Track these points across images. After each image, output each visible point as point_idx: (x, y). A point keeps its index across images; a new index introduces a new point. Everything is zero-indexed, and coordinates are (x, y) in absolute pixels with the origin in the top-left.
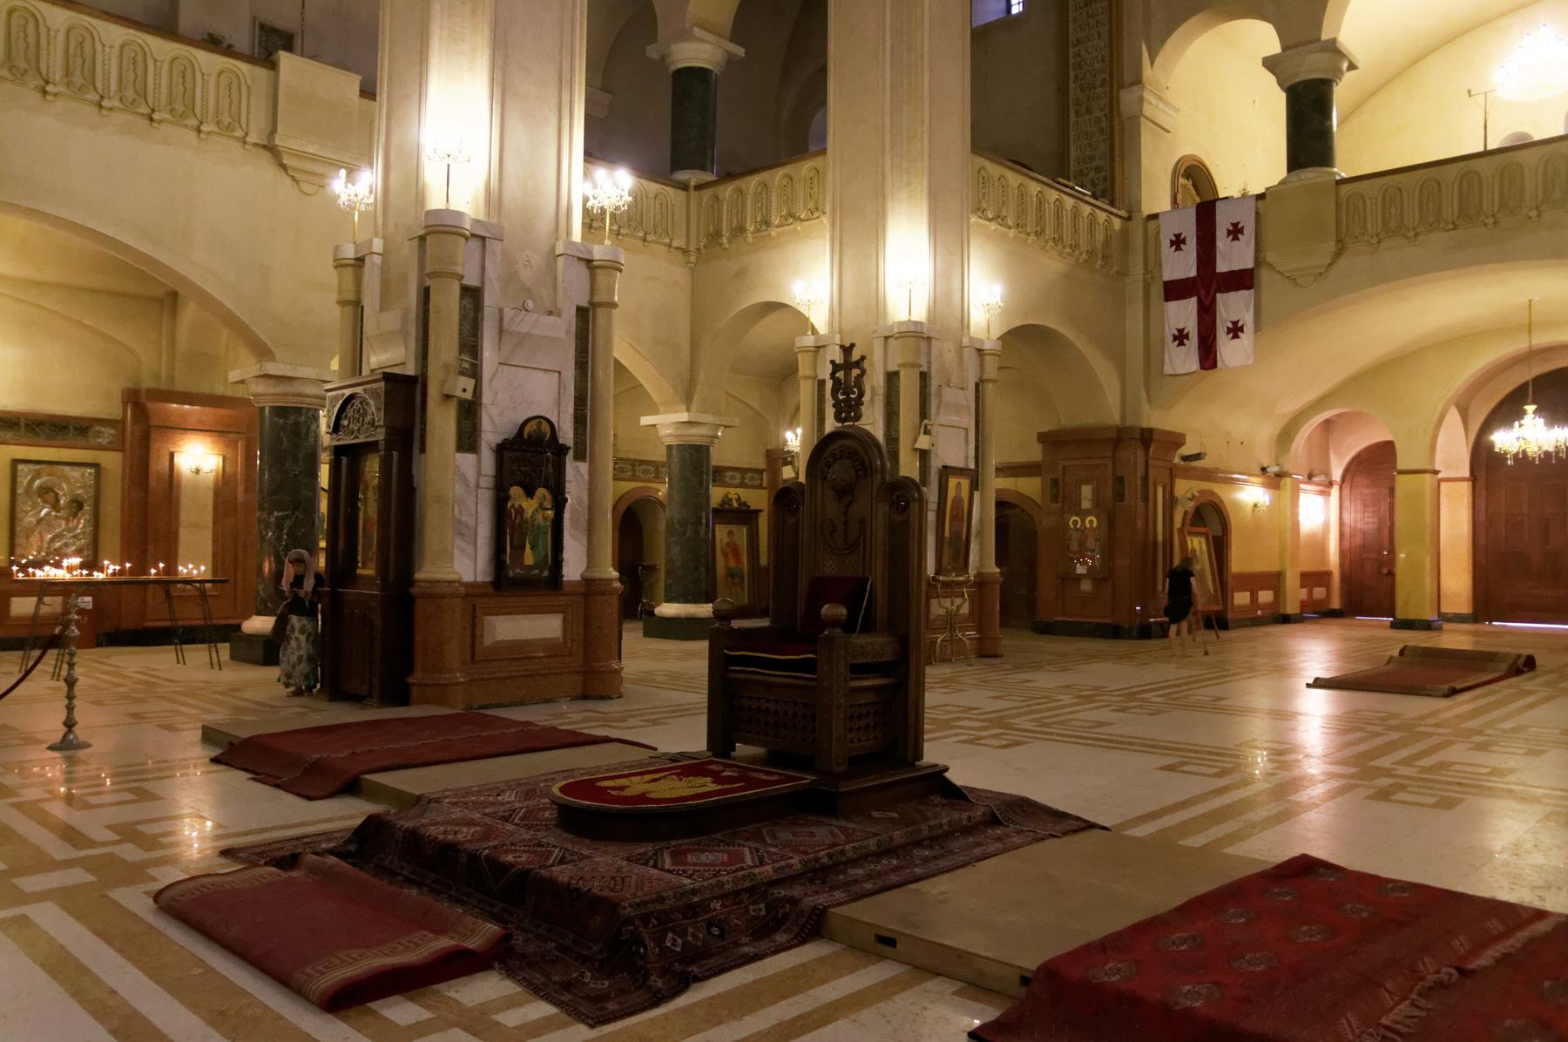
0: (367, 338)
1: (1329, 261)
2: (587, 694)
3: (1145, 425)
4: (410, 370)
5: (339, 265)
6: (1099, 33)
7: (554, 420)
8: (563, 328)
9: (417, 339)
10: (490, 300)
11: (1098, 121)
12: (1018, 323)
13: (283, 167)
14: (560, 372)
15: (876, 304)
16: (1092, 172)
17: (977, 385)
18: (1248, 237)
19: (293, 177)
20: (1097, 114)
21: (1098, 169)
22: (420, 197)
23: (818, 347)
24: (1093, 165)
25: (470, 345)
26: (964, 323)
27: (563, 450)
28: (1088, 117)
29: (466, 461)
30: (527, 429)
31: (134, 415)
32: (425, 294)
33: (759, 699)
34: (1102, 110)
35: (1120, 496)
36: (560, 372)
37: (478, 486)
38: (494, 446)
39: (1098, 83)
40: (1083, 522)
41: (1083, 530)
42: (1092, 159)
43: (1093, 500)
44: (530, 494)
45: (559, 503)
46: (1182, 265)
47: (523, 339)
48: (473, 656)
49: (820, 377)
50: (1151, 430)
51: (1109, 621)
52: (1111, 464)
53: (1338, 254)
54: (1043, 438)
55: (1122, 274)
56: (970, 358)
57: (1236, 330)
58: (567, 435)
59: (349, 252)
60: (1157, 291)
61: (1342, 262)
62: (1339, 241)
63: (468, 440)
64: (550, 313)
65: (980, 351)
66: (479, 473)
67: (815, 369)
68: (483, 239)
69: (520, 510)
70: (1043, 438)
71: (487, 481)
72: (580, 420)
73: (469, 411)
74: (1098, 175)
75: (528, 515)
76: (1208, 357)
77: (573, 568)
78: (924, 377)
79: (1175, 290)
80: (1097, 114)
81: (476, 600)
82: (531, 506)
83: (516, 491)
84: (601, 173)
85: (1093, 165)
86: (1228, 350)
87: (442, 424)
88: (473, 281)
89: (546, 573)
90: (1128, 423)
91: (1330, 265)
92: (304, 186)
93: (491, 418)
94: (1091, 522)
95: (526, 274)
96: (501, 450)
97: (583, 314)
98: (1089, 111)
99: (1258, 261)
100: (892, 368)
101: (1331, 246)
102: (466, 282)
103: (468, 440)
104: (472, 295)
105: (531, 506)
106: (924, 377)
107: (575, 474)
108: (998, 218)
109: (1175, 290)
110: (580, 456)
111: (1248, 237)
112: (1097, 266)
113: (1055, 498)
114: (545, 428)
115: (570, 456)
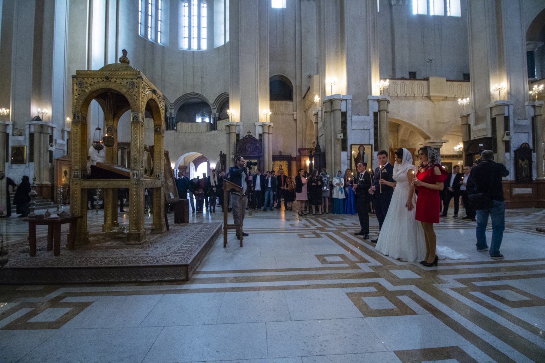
0: (474, 131)
4: (489, 135)
5: (462, 117)
7: (528, 143)
8: (528, 122)
9: (491, 129)
10: (511, 118)
13: (430, 100)
14: (528, 133)
19: (432, 101)
25: (507, 128)
27: (531, 150)
29: (507, 155)
30: (522, 146)
31: (392, 154)
32: (493, 120)
36: (528, 133)
37: (510, 160)
38: (514, 150)
44: (523, 160)
45: (531, 162)
48: (511, 197)
58: (531, 146)
59: (465, 114)
63: (508, 149)
64: (525, 119)
66: (510, 156)
68: (508, 105)
69: (521, 164)
73: (507, 144)
81: (512, 185)
83: (520, 160)
87: (501, 147)
88: (506, 115)
92: (435, 103)
93: (513, 144)
96: (515, 152)
102: (505, 115)
103: (508, 149)
104: (507, 119)
105: (523, 164)
107: (534, 155)
110: (534, 152)
115: (532, 151)
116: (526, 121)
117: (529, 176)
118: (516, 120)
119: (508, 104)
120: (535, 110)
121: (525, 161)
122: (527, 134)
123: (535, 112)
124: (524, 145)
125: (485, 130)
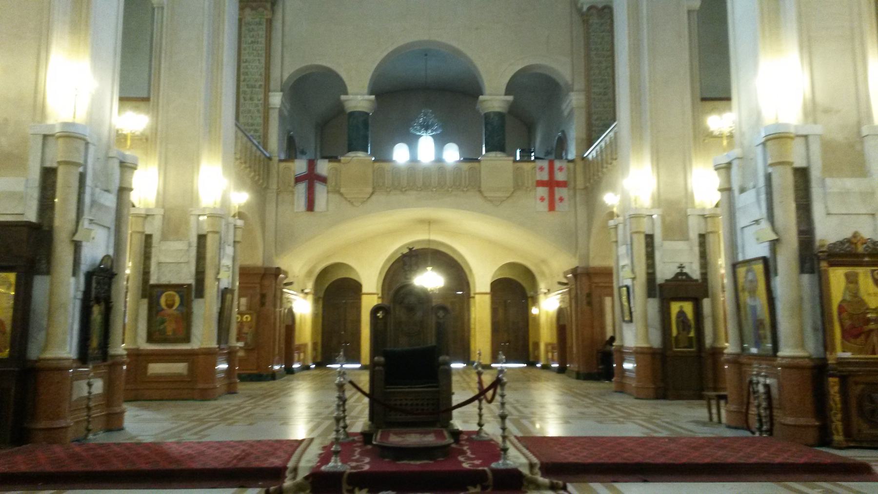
1: (369, 196)
2: (109, 430)
3: (277, 267)
6: (259, 60)
11: (257, 106)
15: (191, 197)
20: (256, 102)
21: (256, 131)
22: (39, 109)
23: (148, 215)
24: (253, 128)
32: (48, 175)
33: (406, 400)
35: (263, 304)
38: (85, 272)
39: (257, 86)
42: (252, 125)
49: (148, 232)
51: (255, 372)
52: (258, 286)
53: (373, 193)
55: (267, 188)
61: (374, 197)
62: (374, 188)
66: (77, 289)
67: (143, 226)
71: (80, 295)
74: (256, 134)
80: (256, 102)
85: (253, 128)
90: (267, 265)
91: (369, 198)
94: (247, 318)
96: (89, 275)
98: (251, 99)
101: (370, 190)
125: (21, 197)
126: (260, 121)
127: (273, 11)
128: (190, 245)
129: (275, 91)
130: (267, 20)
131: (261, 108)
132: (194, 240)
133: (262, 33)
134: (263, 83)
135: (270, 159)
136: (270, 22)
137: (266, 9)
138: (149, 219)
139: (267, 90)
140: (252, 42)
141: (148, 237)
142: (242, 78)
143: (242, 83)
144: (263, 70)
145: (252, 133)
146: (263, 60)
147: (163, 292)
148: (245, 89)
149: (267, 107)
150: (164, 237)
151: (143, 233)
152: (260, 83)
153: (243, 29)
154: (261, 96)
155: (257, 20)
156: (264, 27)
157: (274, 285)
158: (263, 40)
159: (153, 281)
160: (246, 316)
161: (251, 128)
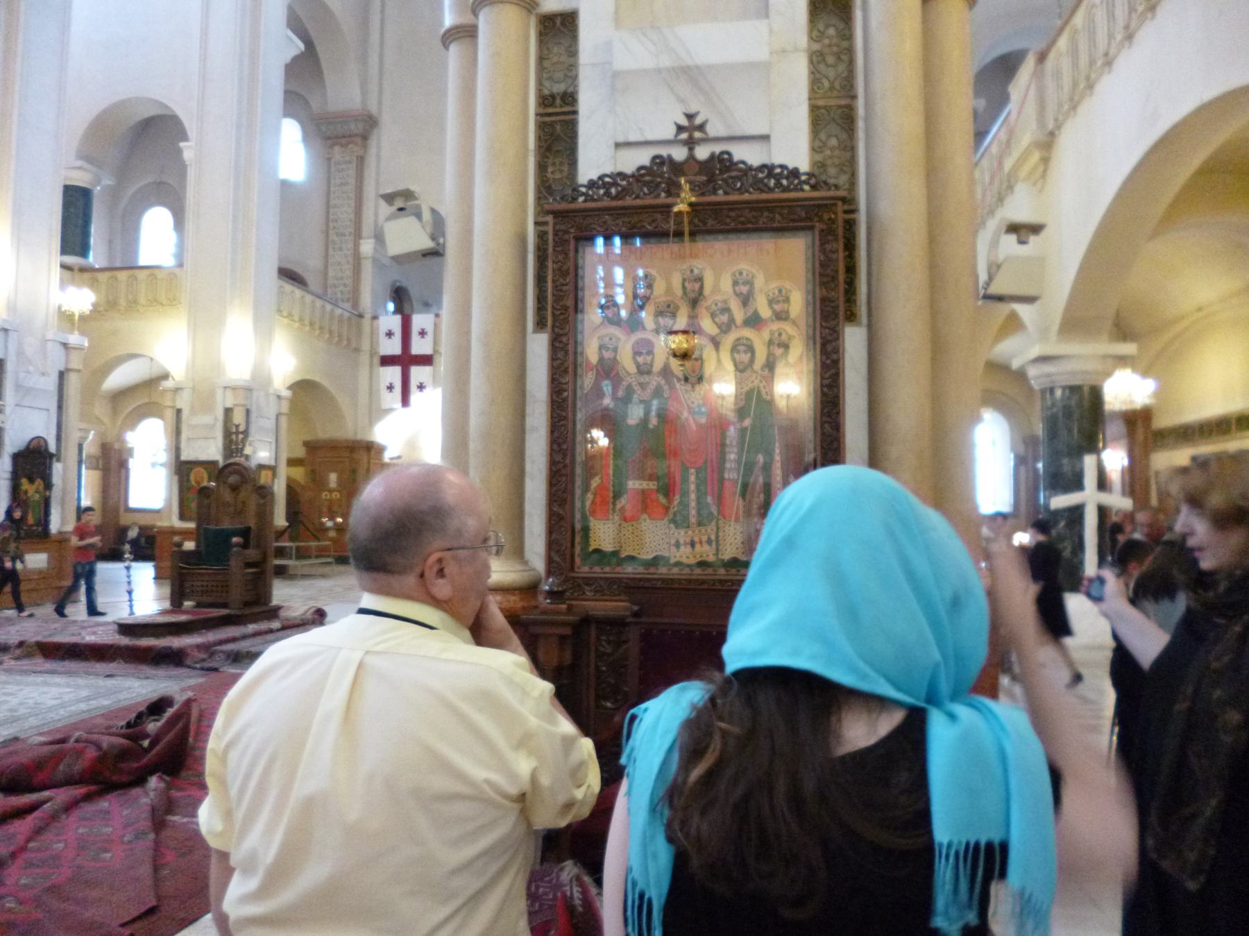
6: (349, 204)
7: (45, 437)
8: (51, 383)
11: (346, 256)
12: (298, 378)
14: (48, 410)
16: (342, 286)
17: (277, 416)
18: (429, 338)
20: (346, 252)
21: (345, 285)
26: (269, 381)
27: (51, 456)
28: (340, 253)
34: (349, 250)
38: (11, 454)
39: (347, 234)
40: (331, 495)
41: (331, 501)
42: (342, 278)
43: (337, 482)
44: (31, 480)
45: (48, 486)
46: (393, 347)
47: (29, 391)
49: (179, 407)
50: (372, 442)
54: (307, 444)
56: (272, 399)
57: (421, 387)
58: (52, 448)
60: (377, 361)
64: (43, 374)
65: (279, 397)
67: (174, 402)
69: (26, 492)
70: (307, 444)
72: (59, 438)
75: (30, 494)
76: (405, 401)
77: (55, 526)
78: (248, 412)
79: (387, 361)
82: (31, 489)
83: (24, 481)
84: (72, 290)
86: (415, 396)
89: (40, 529)
90: (359, 437)
94: (336, 495)
95: (29, 351)
97: (62, 375)
99: (436, 351)
100: (229, 405)
105: (31, 489)
106: (248, 412)
107: (57, 468)
108: (290, 316)
109: (387, 361)
110: (58, 460)
111: (429, 338)
112: (343, 345)
113: (314, 480)
114: (42, 443)
115: (54, 459)
116: (43, 379)
117: (43, 522)
118: (22, 375)
119: (9, 327)
120: (67, 355)
121: (37, 483)
122: (43, 414)
123: (67, 361)
124: (35, 442)
126: (349, 273)
127: (365, 147)
128: (216, 419)
129: (369, 238)
130: (357, 157)
131: (351, 259)
132: (220, 414)
133: (352, 172)
134: (352, 231)
135: (361, 316)
136: (361, 160)
137: (356, 144)
138: (180, 392)
139: (358, 235)
140: (342, 184)
141: (179, 411)
142: (331, 225)
143: (331, 232)
144: (352, 216)
145: (341, 288)
146: (353, 204)
147: (191, 469)
148: (335, 238)
149: (357, 259)
150: (193, 412)
151: (173, 407)
152: (350, 230)
153: (333, 169)
154: (351, 245)
155: (347, 158)
156: (354, 165)
157: (365, 460)
158: (352, 181)
159: (184, 457)
160: (335, 493)
161: (340, 282)
